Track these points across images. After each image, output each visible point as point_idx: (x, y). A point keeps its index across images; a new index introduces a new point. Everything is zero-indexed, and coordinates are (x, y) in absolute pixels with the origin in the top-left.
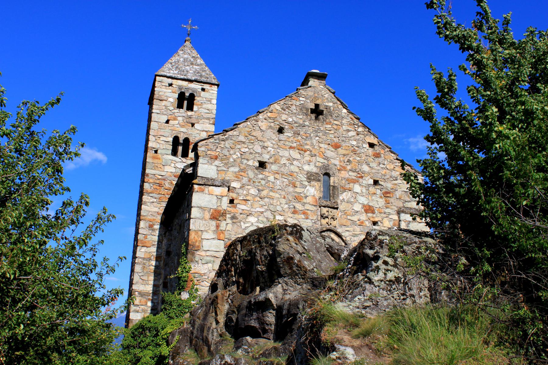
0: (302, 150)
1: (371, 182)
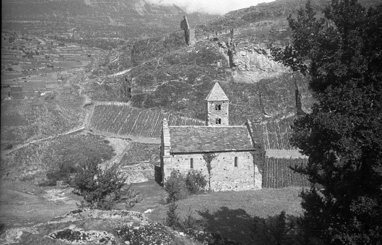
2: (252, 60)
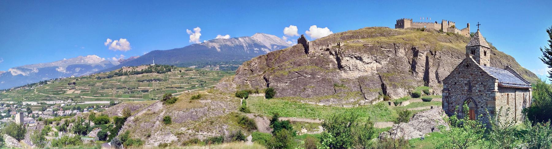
0: (464, 77)
1: (481, 83)
2: (353, 64)
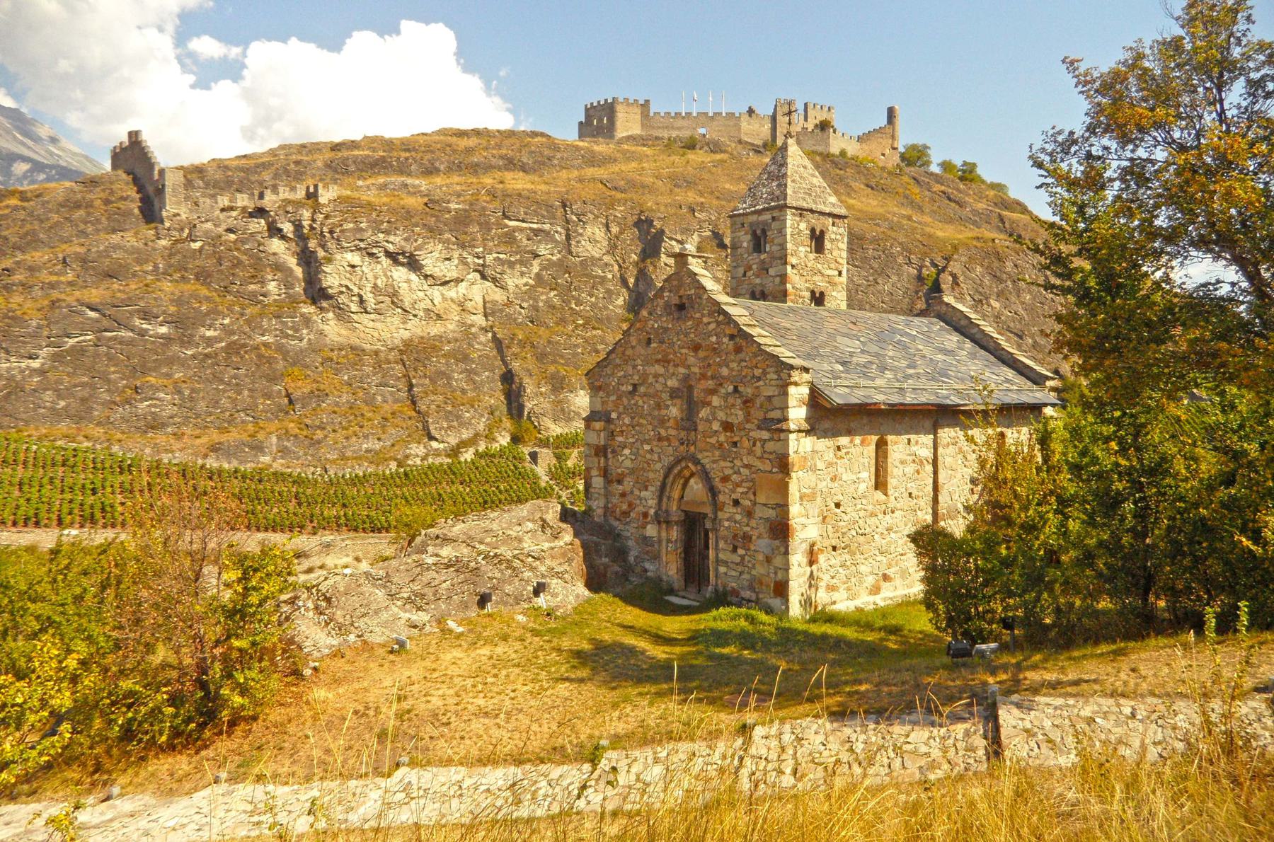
0: (665, 361)
1: (731, 388)
2: (379, 282)
